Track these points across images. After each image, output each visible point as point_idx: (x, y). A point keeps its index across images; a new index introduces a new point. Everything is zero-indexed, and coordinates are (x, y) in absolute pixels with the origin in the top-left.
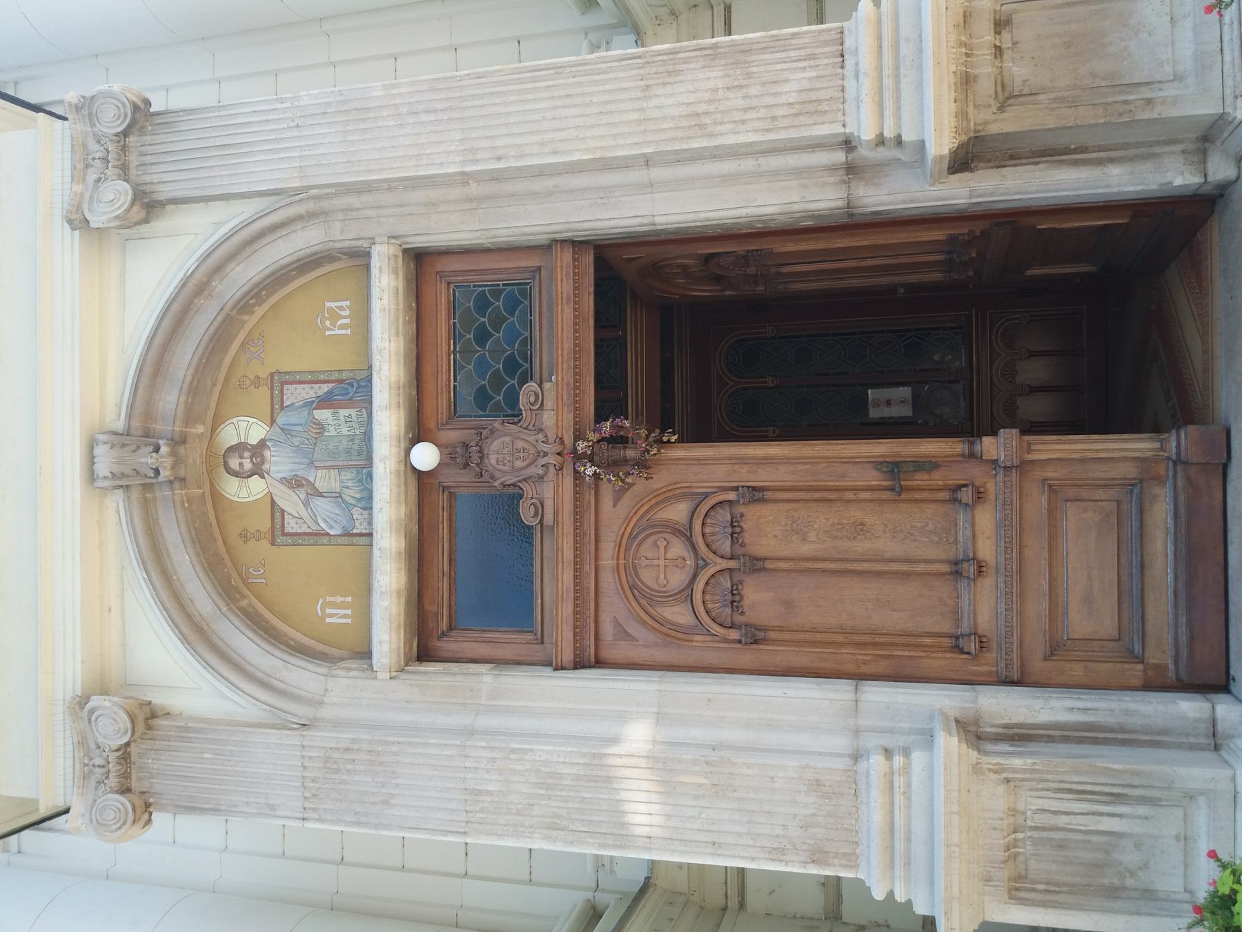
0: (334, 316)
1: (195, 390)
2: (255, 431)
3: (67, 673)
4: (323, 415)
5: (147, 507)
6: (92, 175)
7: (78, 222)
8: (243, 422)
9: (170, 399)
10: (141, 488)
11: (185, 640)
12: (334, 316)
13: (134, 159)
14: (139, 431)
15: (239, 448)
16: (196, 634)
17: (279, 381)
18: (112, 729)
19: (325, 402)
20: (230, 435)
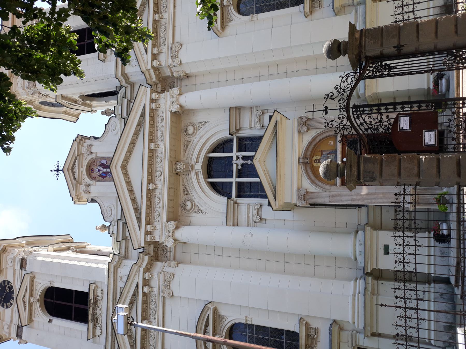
0: (331, 143)
1: (312, 152)
2: (319, 157)
3: (295, 187)
4: (328, 155)
5: (305, 166)
6: (301, 126)
7: (300, 132)
8: (317, 156)
9: (309, 153)
10: (305, 164)
11: (311, 182)
12: (331, 143)
13: (307, 124)
14: (305, 157)
15: (316, 160)
16: (312, 182)
17: (322, 151)
18: (303, 193)
19: (329, 154)
20: (315, 158)
